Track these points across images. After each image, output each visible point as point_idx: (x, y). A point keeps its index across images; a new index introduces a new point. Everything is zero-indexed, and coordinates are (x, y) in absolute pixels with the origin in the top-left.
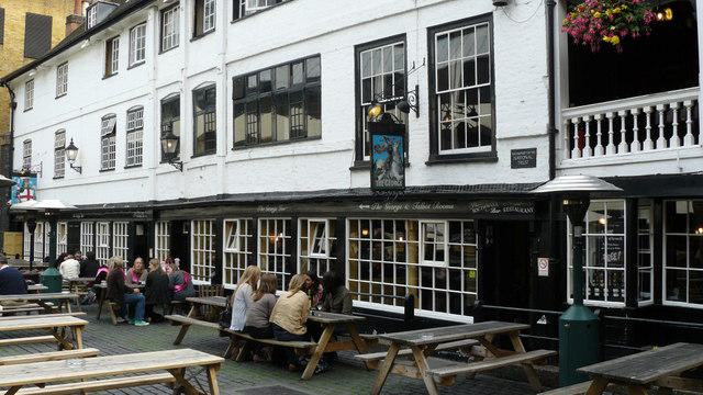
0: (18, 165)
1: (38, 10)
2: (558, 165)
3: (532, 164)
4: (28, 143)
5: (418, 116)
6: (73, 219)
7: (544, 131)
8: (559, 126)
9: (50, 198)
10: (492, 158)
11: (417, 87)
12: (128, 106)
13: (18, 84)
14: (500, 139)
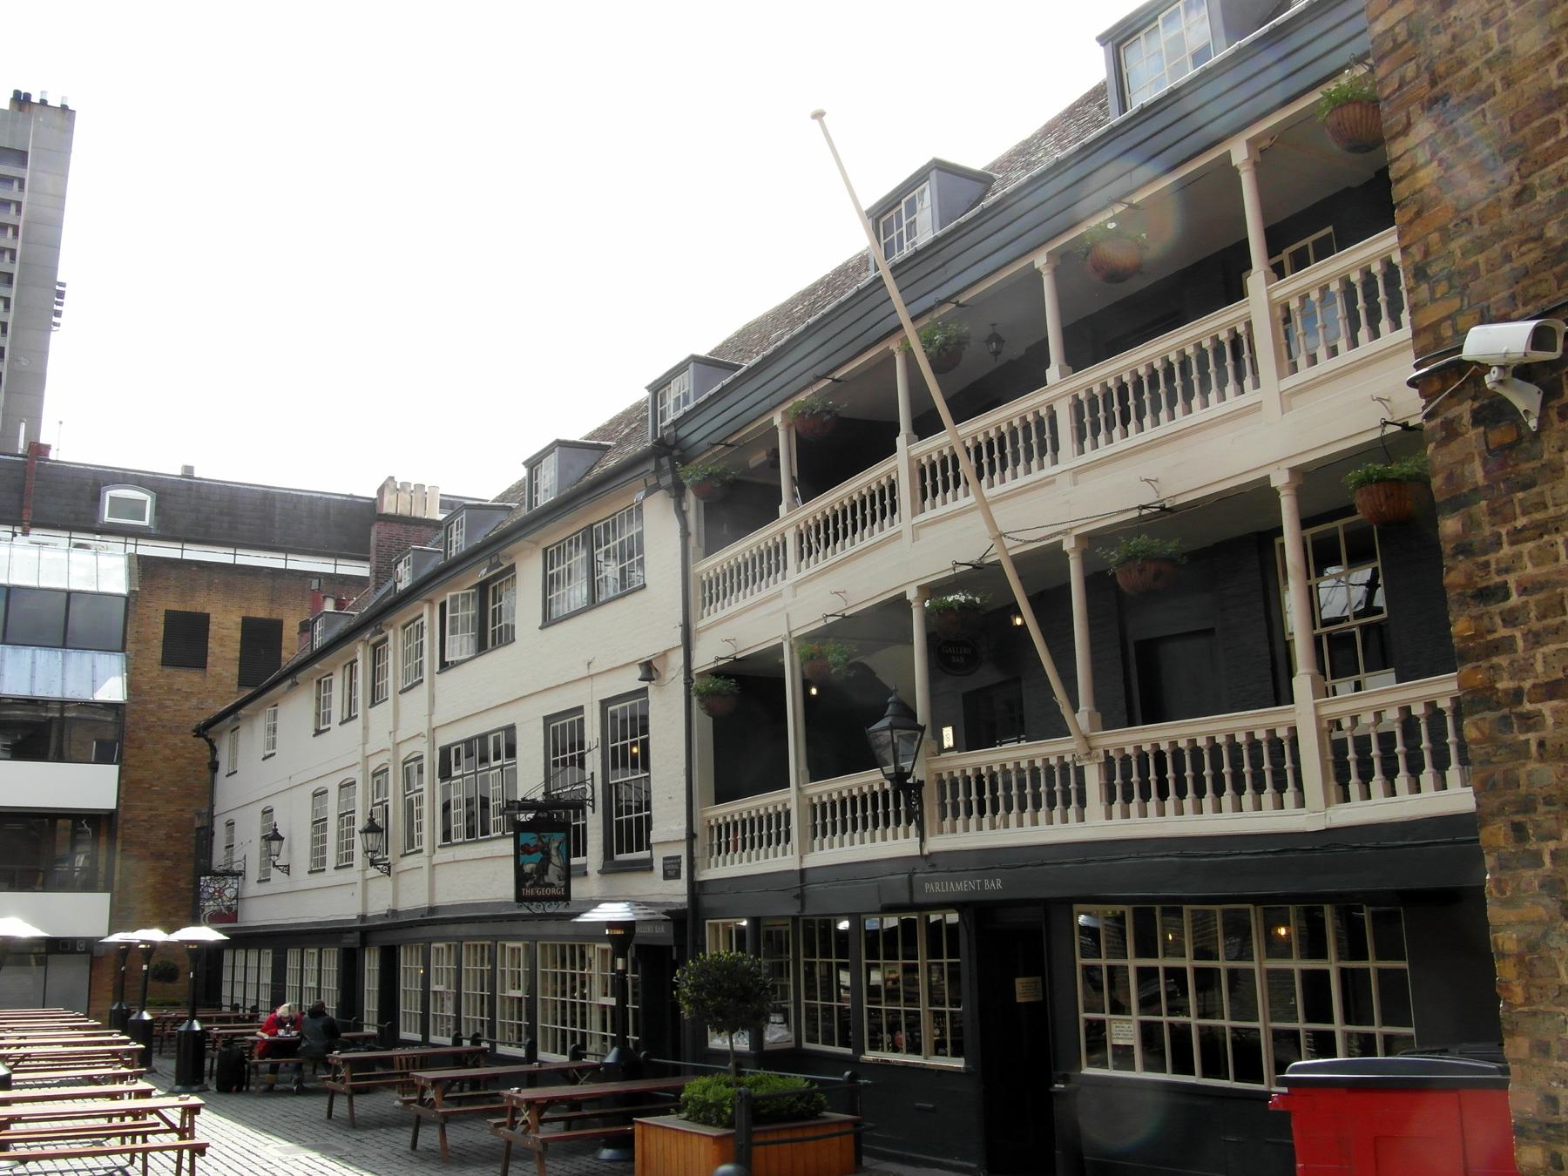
0: (219, 859)
1: (260, 611)
3: (677, 876)
4: (230, 824)
5: (594, 812)
7: (683, 836)
8: (697, 829)
9: (262, 912)
10: (646, 866)
11: (592, 774)
12: (340, 778)
13: (220, 733)
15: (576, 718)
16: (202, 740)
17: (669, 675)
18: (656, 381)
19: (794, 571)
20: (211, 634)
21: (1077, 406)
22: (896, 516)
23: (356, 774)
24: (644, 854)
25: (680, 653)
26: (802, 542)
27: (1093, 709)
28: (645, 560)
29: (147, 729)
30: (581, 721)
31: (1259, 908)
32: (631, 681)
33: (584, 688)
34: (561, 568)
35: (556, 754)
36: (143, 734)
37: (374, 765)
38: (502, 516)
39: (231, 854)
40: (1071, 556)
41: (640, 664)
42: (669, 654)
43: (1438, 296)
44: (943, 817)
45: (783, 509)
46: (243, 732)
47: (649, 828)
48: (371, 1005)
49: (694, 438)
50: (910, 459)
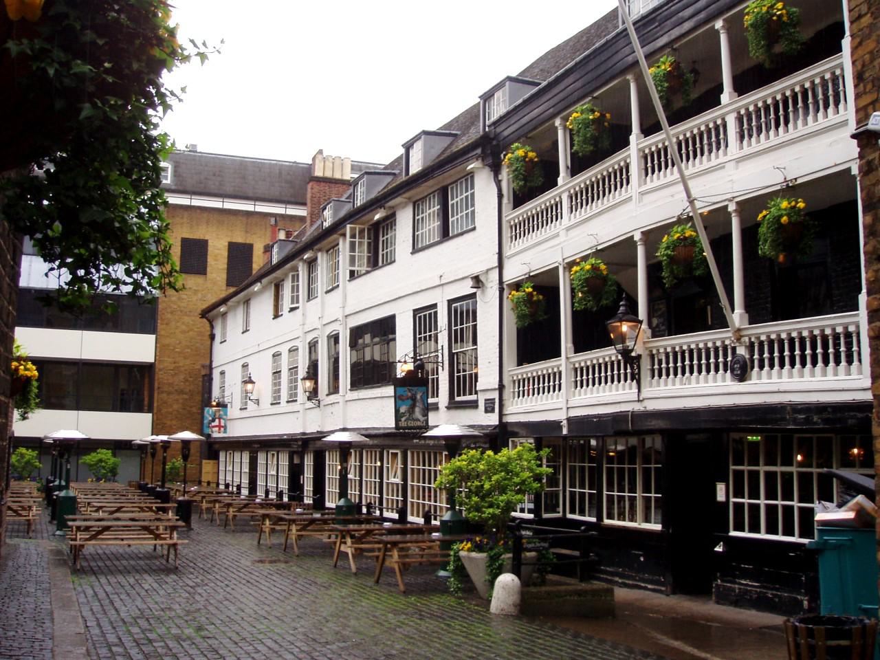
0: (216, 393)
1: (239, 238)
2: (505, 412)
3: (493, 411)
4: (222, 373)
6: (255, 446)
7: (497, 387)
8: (506, 382)
9: (240, 429)
10: (473, 405)
13: (216, 317)
14: (481, 391)
15: (432, 311)
16: (205, 320)
17: (489, 285)
18: (485, 93)
19: (567, 219)
20: (209, 253)
21: (740, 119)
22: (629, 186)
23: (296, 343)
24: (473, 397)
25: (497, 270)
26: (572, 202)
27: (743, 311)
28: (476, 211)
29: (172, 313)
30: (436, 313)
31: (839, 436)
32: (466, 288)
33: (438, 291)
34: (424, 215)
35: (420, 334)
36: (169, 316)
37: (310, 337)
38: (389, 179)
39: (223, 391)
40: (733, 215)
41: (472, 278)
42: (490, 272)
43: (867, 90)
44: (653, 377)
45: (560, 181)
46: (230, 317)
47: (476, 381)
48: (308, 487)
49: (506, 133)
50: (639, 150)
